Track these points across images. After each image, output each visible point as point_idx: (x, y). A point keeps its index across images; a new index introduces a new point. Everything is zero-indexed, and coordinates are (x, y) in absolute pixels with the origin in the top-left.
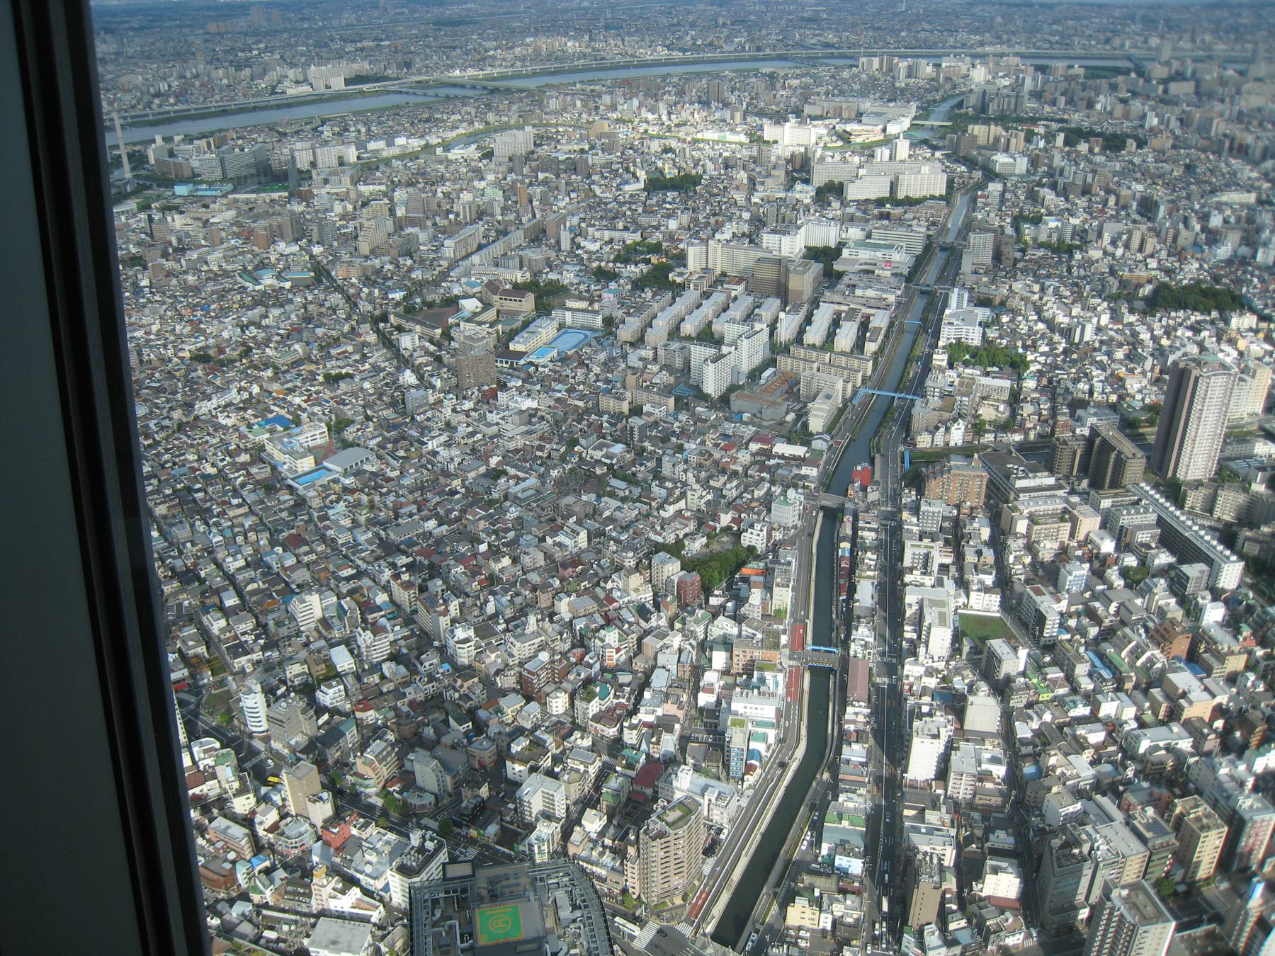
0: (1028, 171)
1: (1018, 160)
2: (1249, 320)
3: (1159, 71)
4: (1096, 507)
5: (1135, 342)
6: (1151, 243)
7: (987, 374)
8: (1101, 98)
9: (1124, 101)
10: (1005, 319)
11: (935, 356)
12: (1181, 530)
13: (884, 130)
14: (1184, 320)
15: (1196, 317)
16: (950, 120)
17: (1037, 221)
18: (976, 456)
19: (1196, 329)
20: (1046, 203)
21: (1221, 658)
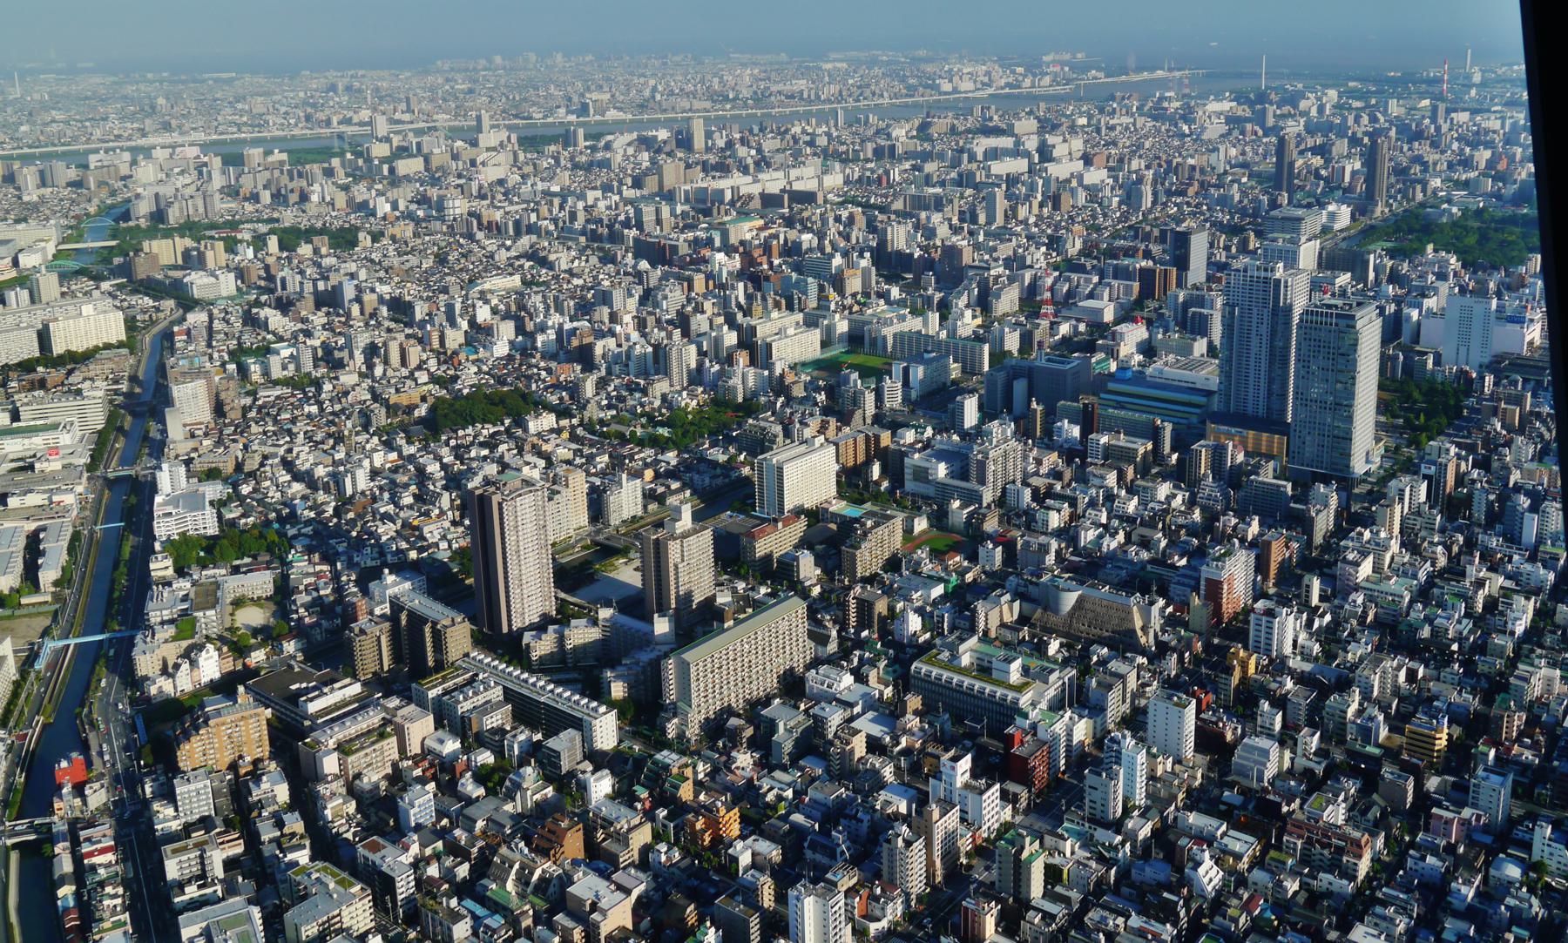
0: (239, 289)
1: (222, 277)
2: (548, 421)
3: (380, 150)
4: (422, 703)
5: (422, 476)
6: (415, 354)
7: (236, 570)
8: (316, 187)
9: (346, 188)
10: (245, 489)
11: (152, 566)
12: (534, 696)
13: (15, 263)
14: (475, 437)
15: (488, 430)
16: (114, 237)
17: (265, 351)
18: (241, 689)
19: (490, 445)
20: (271, 327)
21: (623, 839)
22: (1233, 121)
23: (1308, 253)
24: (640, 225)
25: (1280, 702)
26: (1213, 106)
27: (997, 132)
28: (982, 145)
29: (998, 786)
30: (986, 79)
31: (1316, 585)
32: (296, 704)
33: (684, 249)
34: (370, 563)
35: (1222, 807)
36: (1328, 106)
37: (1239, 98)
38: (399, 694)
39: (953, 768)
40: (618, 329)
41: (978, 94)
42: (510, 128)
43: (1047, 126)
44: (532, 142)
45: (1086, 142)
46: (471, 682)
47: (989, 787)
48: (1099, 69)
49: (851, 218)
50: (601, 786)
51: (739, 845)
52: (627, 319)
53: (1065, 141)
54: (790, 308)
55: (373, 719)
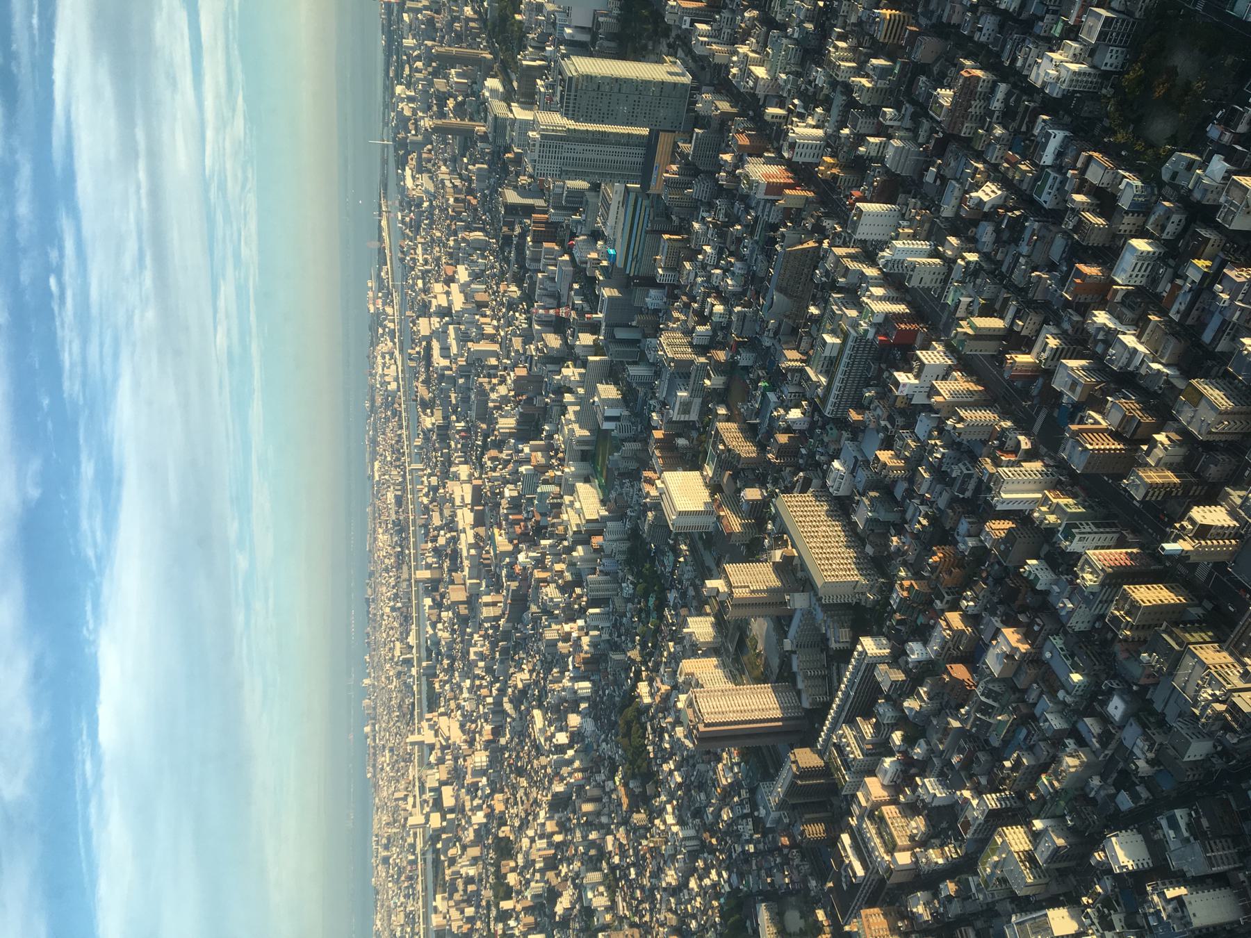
3: (436, 821)
8: (463, 871)
9: (464, 848)
10: (693, 925)
22: (420, 169)
23: (519, 113)
24: (497, 619)
25: (860, 139)
26: (409, 183)
27: (428, 349)
28: (439, 361)
29: (918, 352)
30: (387, 357)
31: (772, 110)
32: (859, 885)
33: (514, 585)
34: (750, 826)
35: (938, 182)
36: (408, 93)
37: (402, 163)
38: (849, 805)
39: (904, 385)
40: (575, 635)
41: (399, 363)
42: (421, 719)
43: (424, 310)
44: (433, 702)
45: (437, 281)
46: (840, 748)
47: (918, 359)
48: (380, 270)
49: (493, 459)
50: (916, 652)
51: (961, 546)
52: (567, 628)
53: (435, 297)
54: (559, 505)
55: (870, 829)
